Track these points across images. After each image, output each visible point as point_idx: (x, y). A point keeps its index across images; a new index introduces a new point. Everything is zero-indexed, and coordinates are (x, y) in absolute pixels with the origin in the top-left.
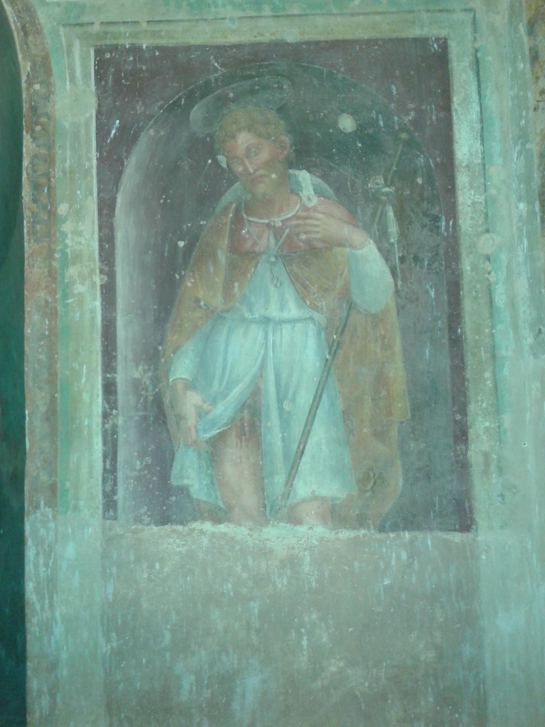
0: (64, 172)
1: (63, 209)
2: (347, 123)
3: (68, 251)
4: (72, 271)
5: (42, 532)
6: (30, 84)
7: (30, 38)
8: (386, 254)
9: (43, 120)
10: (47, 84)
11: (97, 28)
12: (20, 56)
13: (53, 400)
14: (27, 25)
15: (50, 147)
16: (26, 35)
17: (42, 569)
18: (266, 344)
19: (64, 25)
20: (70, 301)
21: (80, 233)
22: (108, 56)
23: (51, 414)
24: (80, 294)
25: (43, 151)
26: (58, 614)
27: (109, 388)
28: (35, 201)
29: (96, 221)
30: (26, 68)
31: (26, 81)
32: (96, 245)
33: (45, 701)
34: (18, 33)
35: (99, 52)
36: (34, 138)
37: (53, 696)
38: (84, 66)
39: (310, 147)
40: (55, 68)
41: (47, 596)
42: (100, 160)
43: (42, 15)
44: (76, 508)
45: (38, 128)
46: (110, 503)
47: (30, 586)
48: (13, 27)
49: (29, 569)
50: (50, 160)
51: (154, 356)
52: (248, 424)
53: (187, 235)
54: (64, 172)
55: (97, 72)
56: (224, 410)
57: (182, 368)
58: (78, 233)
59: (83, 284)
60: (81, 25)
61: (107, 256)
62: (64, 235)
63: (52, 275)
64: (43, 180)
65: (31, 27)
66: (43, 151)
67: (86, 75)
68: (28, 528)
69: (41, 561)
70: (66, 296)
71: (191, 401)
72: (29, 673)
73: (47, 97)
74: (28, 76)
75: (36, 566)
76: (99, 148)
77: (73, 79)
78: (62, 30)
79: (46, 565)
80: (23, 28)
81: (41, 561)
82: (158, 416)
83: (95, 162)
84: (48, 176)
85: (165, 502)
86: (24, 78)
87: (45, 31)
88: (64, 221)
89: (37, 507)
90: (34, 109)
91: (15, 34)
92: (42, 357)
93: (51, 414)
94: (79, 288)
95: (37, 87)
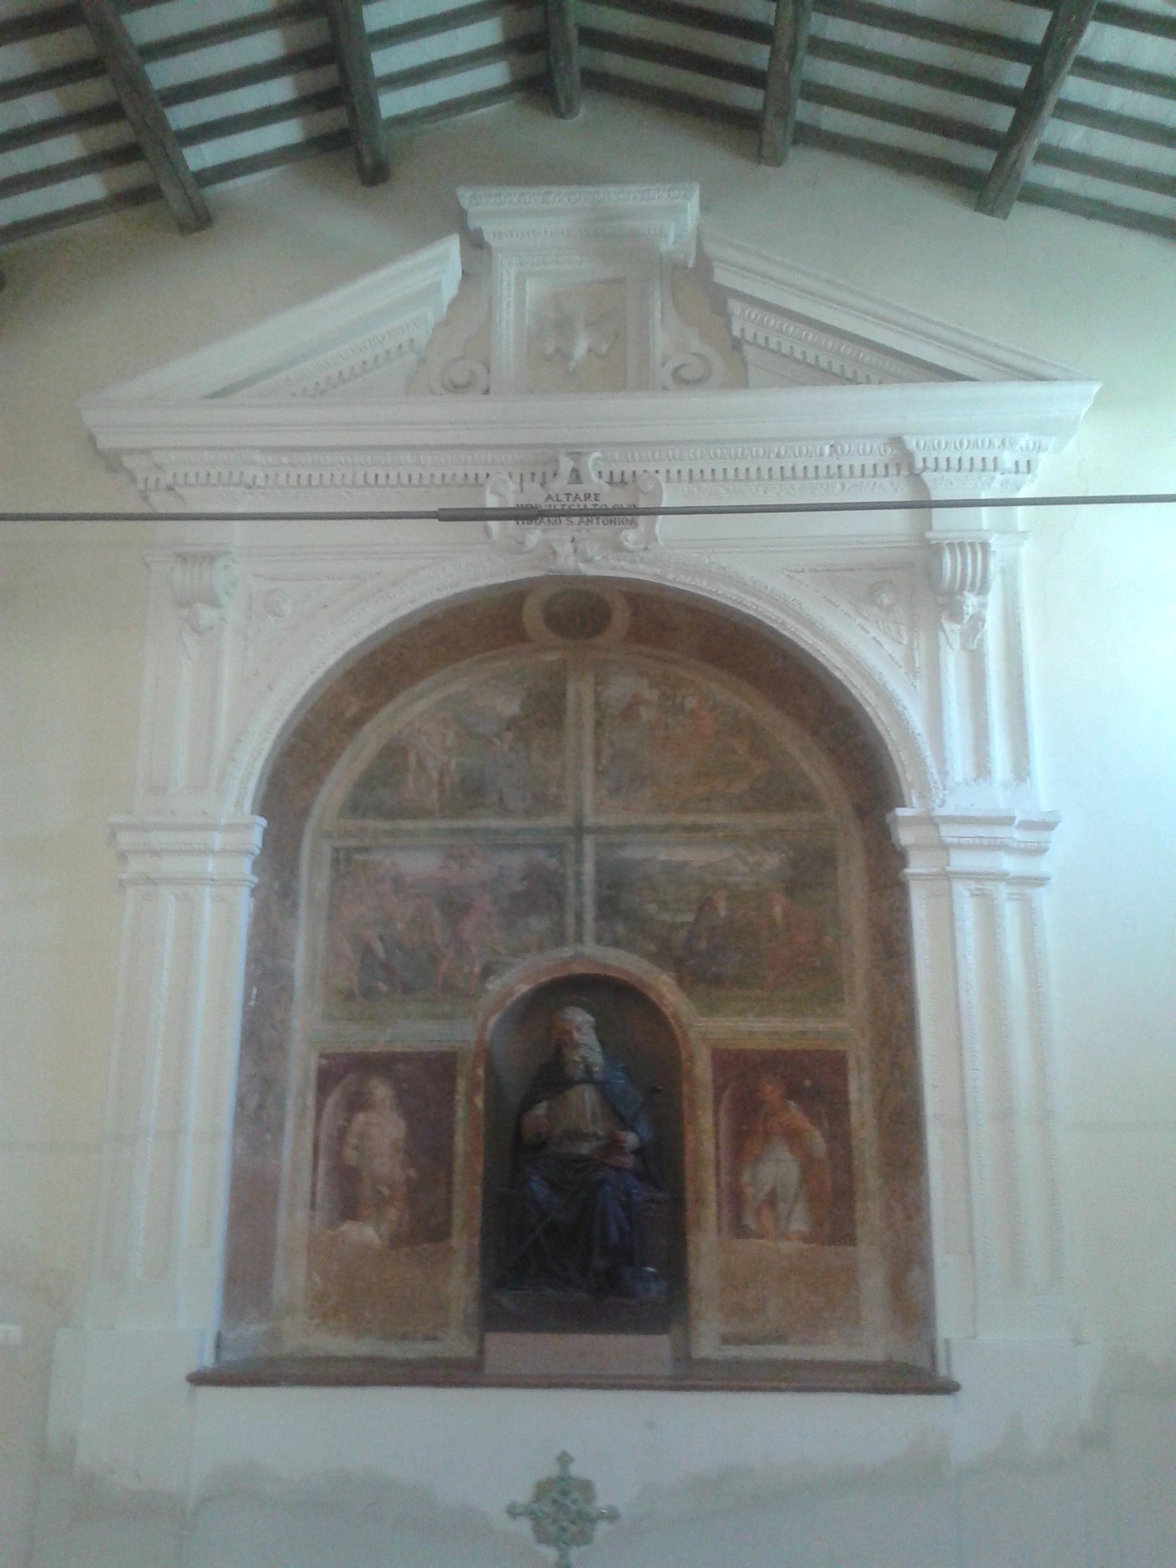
2: (808, 1083)
8: (823, 1135)
18: (778, 1169)
21: (706, 1120)
27: (718, 1185)
39: (793, 1091)
46: (720, 1229)
51: (735, 1173)
52: (772, 1200)
53: (747, 1128)
56: (762, 1195)
57: (746, 1177)
61: (717, 1132)
71: (750, 1191)
82: (736, 1198)
85: (740, 1230)
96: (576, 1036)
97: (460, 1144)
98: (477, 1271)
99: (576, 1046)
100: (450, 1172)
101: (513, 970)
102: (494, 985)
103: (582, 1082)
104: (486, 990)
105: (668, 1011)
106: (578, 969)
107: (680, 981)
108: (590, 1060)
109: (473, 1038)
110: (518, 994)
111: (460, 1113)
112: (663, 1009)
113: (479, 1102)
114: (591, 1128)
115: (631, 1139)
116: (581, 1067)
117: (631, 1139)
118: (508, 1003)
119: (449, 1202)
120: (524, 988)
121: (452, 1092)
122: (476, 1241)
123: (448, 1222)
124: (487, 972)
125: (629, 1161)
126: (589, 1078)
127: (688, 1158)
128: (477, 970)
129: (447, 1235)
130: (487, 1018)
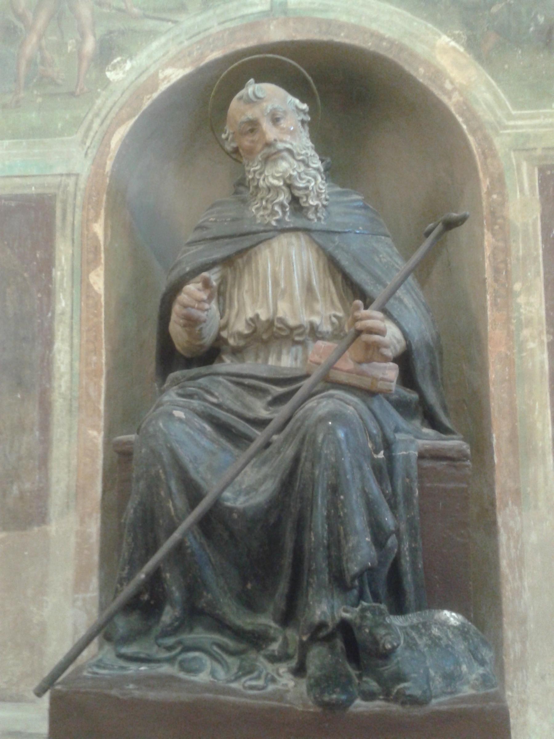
0: (518, 259)
1: (517, 287)
3: (523, 317)
4: (526, 332)
5: (511, 523)
6: (489, 194)
7: (489, 160)
9: (500, 221)
10: (502, 194)
11: (539, 152)
12: (481, 175)
13: (514, 429)
14: (486, 151)
15: (506, 240)
16: (486, 158)
17: (513, 551)
19: (515, 150)
20: (524, 354)
22: (549, 173)
23: (513, 439)
24: (531, 349)
25: (501, 244)
26: (526, 584)
28: (496, 280)
29: (543, 295)
30: (485, 184)
31: (486, 193)
32: (543, 313)
33: (518, 647)
34: (479, 157)
35: (542, 170)
36: (494, 235)
37: (523, 643)
38: (531, 180)
40: (508, 182)
41: (517, 570)
42: (544, 250)
43: (497, 142)
44: (536, 507)
45: (497, 227)
47: (504, 563)
48: (475, 152)
49: (503, 550)
50: (506, 251)
54: (518, 259)
55: (540, 185)
58: (528, 304)
59: (534, 342)
60: (527, 150)
62: (519, 306)
63: (510, 335)
64: (502, 266)
65: (489, 152)
66: (501, 244)
67: (532, 187)
68: (500, 520)
69: (512, 544)
70: (520, 351)
72: (505, 626)
73: (503, 203)
74: (488, 188)
75: (508, 548)
76: (545, 241)
77: (522, 190)
78: (512, 154)
79: (516, 548)
80: (483, 153)
81: (512, 544)
83: (541, 252)
84: (505, 262)
86: (484, 190)
87: (500, 155)
88: (518, 295)
89: (506, 505)
90: (493, 213)
91: (477, 158)
92: (505, 395)
93: (513, 439)
94: (531, 345)
95: (495, 196)
96: (271, 132)
97: (63, 356)
98: (95, 582)
99: (271, 155)
100: (46, 407)
101: (155, 45)
102: (120, 74)
104: (107, 83)
105: (451, 103)
106: (276, 34)
107: (473, 45)
109: (83, 166)
110: (164, 87)
111: (62, 303)
112: (444, 99)
113: (98, 281)
114: (305, 318)
116: (283, 198)
118: (146, 103)
119: (44, 461)
120: (175, 74)
121: (48, 264)
122: (94, 528)
123: (42, 495)
124: (107, 52)
125: (391, 372)
127: (495, 371)
128: (90, 45)
129: (42, 518)
130: (108, 135)
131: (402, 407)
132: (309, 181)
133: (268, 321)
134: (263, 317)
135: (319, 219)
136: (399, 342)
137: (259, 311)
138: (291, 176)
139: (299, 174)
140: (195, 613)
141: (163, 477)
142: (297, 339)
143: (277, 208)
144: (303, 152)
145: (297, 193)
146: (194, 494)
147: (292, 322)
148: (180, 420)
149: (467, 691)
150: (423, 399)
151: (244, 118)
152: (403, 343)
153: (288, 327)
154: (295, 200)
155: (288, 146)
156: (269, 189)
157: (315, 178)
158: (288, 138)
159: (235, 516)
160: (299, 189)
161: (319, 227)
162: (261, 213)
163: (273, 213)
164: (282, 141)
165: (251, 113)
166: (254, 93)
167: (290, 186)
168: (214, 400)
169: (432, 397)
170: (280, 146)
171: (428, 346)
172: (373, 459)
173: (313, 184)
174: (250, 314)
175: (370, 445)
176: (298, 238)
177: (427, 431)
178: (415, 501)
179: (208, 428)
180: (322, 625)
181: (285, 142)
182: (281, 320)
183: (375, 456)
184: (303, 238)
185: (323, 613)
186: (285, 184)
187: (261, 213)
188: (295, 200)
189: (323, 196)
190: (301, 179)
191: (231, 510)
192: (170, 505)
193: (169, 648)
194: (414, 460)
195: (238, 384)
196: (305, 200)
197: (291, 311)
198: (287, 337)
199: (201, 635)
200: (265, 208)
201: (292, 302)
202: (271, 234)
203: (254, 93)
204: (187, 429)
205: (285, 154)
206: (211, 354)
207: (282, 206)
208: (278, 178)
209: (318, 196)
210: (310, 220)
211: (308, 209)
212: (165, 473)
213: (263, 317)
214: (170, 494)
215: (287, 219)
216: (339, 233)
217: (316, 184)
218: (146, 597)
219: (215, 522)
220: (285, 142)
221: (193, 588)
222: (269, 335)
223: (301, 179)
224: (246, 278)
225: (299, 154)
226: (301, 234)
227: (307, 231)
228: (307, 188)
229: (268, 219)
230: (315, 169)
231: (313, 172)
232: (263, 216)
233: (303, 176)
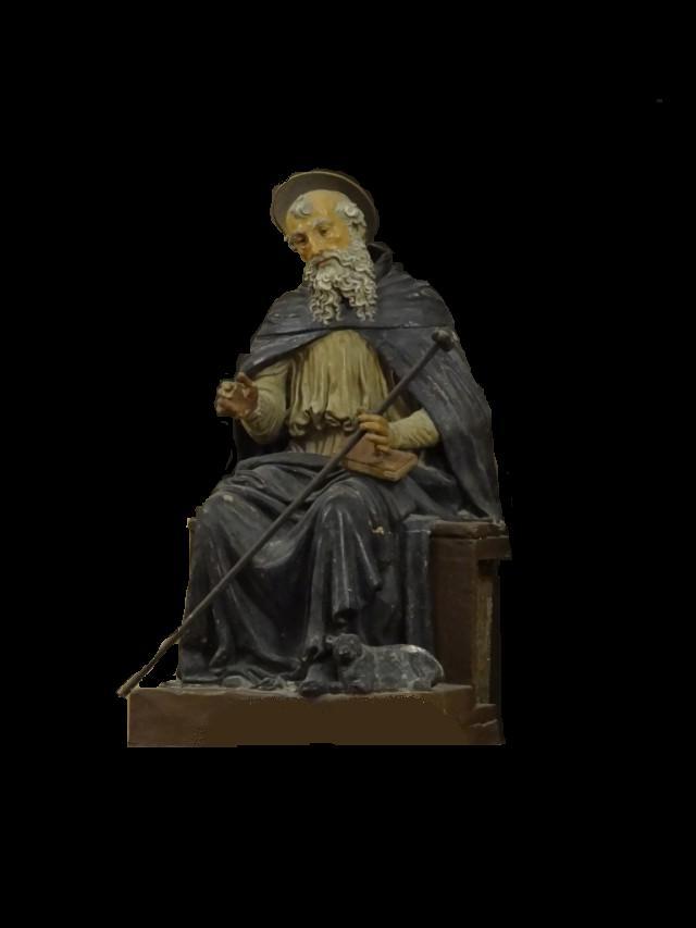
103: (335, 327)
108: (345, 288)
115: (416, 426)
117: (416, 426)
126: (347, 317)
131: (436, 492)
132: (355, 284)
133: (319, 414)
134: (315, 411)
135: (367, 317)
136: (429, 433)
137: (313, 404)
138: (337, 282)
139: (345, 279)
140: (240, 650)
141: (212, 546)
142: (347, 429)
143: (328, 309)
144: (349, 258)
145: (346, 295)
146: (232, 557)
147: (341, 415)
148: (228, 502)
149: (407, 692)
150: (459, 485)
151: (295, 231)
152: (436, 433)
153: (338, 419)
154: (345, 301)
155: (335, 255)
156: (322, 291)
157: (361, 280)
158: (334, 247)
159: (262, 575)
160: (347, 292)
161: (367, 325)
162: (316, 312)
163: (325, 313)
164: (329, 250)
165: (300, 227)
166: (301, 212)
167: (339, 291)
168: (261, 486)
169: (468, 481)
170: (327, 255)
171: (461, 436)
172: (372, 533)
173: (358, 287)
174: (305, 407)
175: (370, 523)
176: (350, 335)
177: (464, 513)
178: (424, 571)
179: (253, 509)
180: (314, 649)
181: (332, 251)
182: (330, 413)
183: (374, 531)
184: (355, 335)
185: (316, 641)
186: (333, 287)
187: (316, 312)
188: (345, 301)
189: (370, 297)
190: (348, 283)
191: (262, 570)
192: (218, 568)
193: (217, 675)
194: (425, 539)
195: (289, 472)
196: (352, 300)
197: (341, 404)
198: (337, 428)
199: (242, 666)
200: (320, 307)
201: (341, 395)
202: (324, 332)
203: (301, 212)
204: (234, 510)
205: (334, 261)
206: (282, 440)
207: (332, 305)
208: (326, 283)
209: (366, 295)
210: (358, 318)
211: (357, 308)
212: (215, 544)
213: (315, 411)
214: (218, 559)
215: (338, 318)
216: (388, 328)
217: (363, 285)
218: (205, 640)
219: (247, 577)
220: (332, 251)
221: (237, 629)
222: (322, 426)
223: (348, 283)
224: (306, 369)
225: (344, 261)
226: (350, 331)
227: (356, 328)
228: (353, 291)
229: (321, 318)
230: (361, 272)
231: (360, 276)
232: (317, 315)
233: (350, 280)
